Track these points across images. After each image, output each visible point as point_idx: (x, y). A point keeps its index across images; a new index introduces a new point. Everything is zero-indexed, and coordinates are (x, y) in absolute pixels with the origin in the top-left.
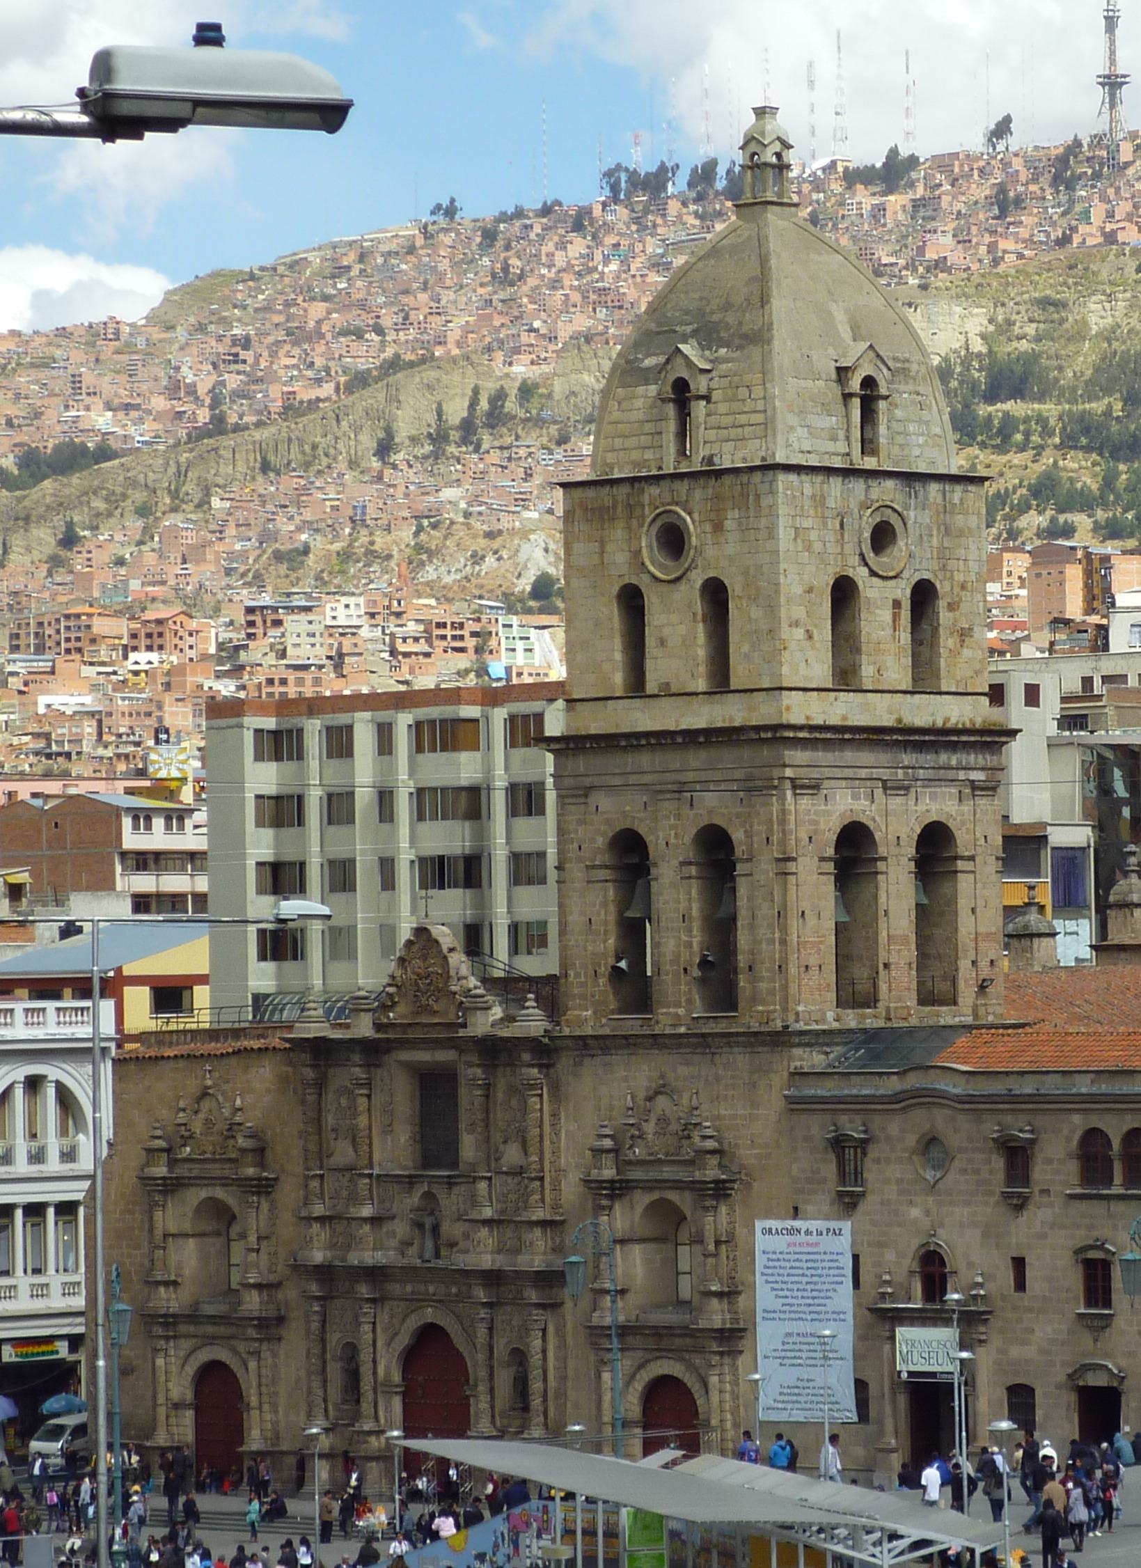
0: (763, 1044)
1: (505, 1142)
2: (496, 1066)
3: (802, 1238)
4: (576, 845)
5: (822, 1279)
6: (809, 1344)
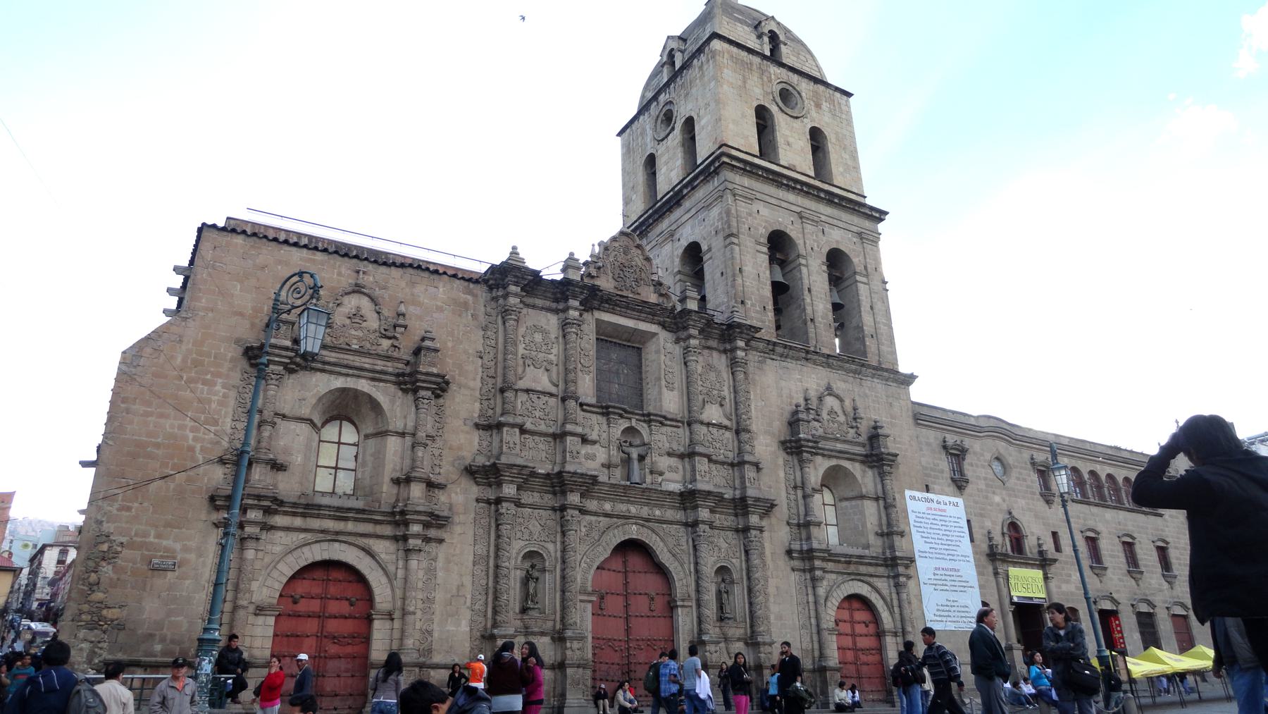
3: (934, 505)
4: (746, 226)
5: (952, 533)
6: (950, 576)
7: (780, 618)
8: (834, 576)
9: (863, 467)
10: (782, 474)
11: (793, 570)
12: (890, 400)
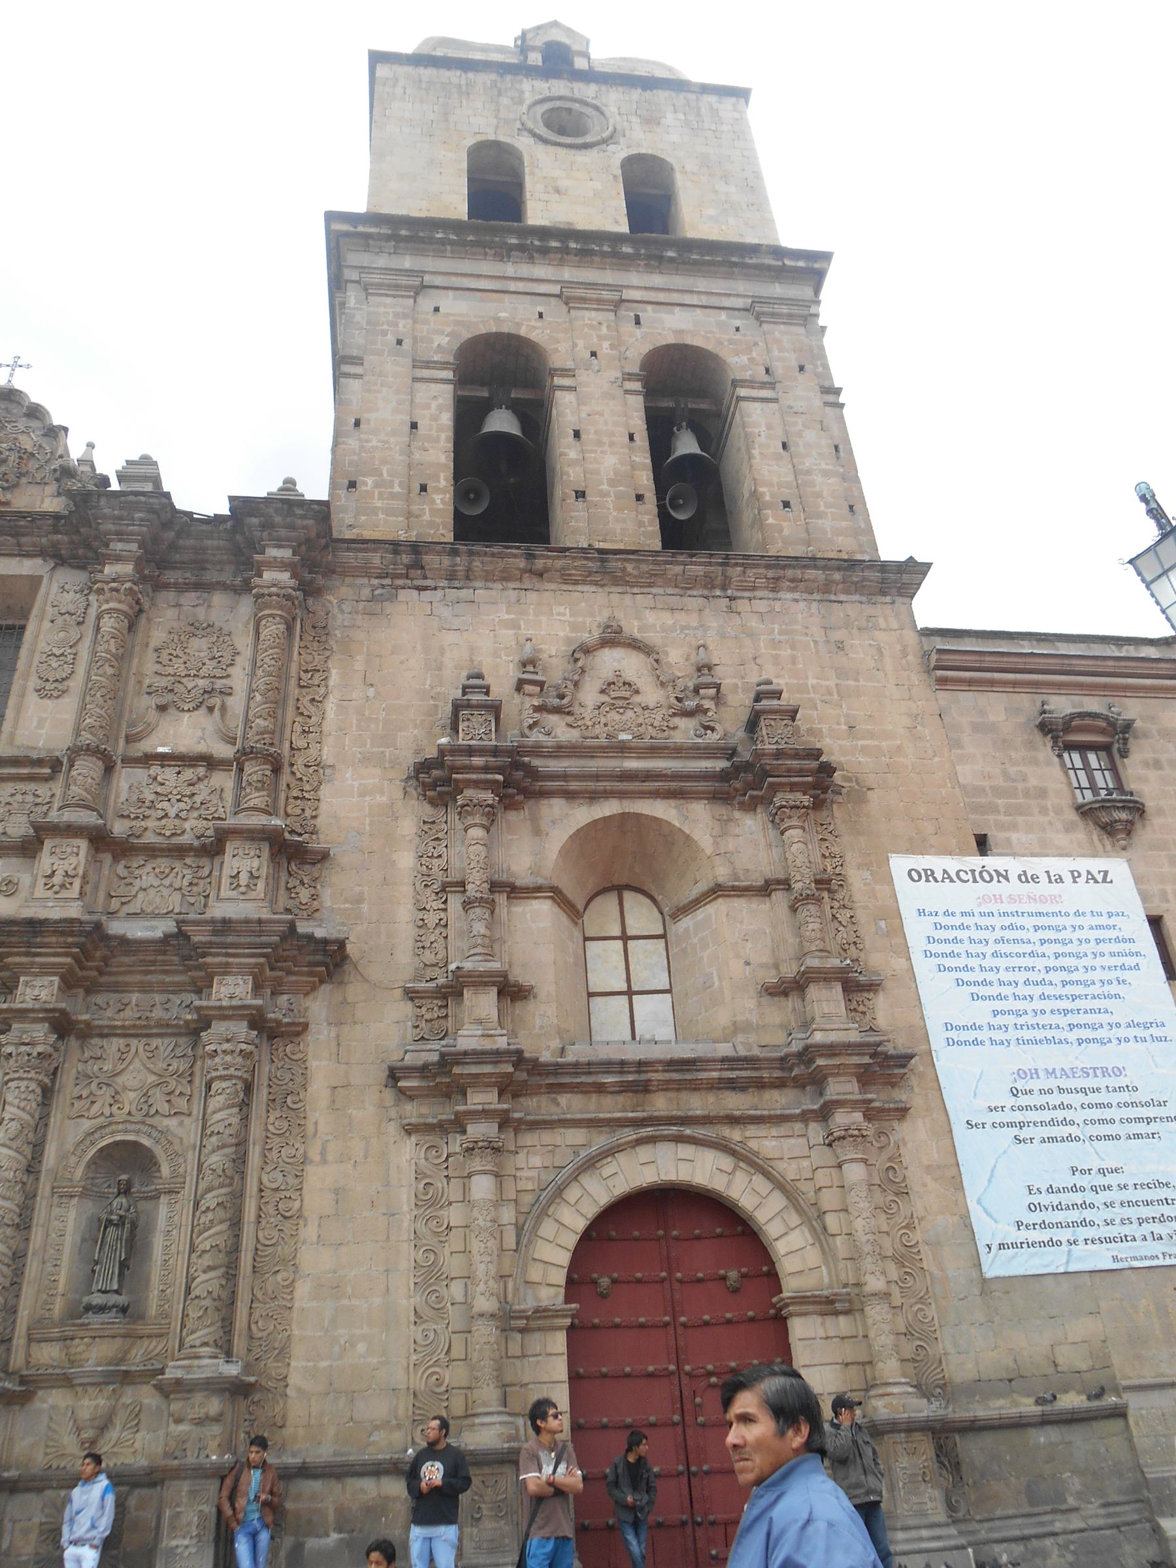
0: (858, 588)
1: (162, 708)
2: (159, 586)
4: (391, 338)
6: (1084, 1091)
7: (334, 1288)
8: (576, 1136)
9: (722, 810)
10: (406, 860)
11: (410, 1130)
12: (838, 635)
